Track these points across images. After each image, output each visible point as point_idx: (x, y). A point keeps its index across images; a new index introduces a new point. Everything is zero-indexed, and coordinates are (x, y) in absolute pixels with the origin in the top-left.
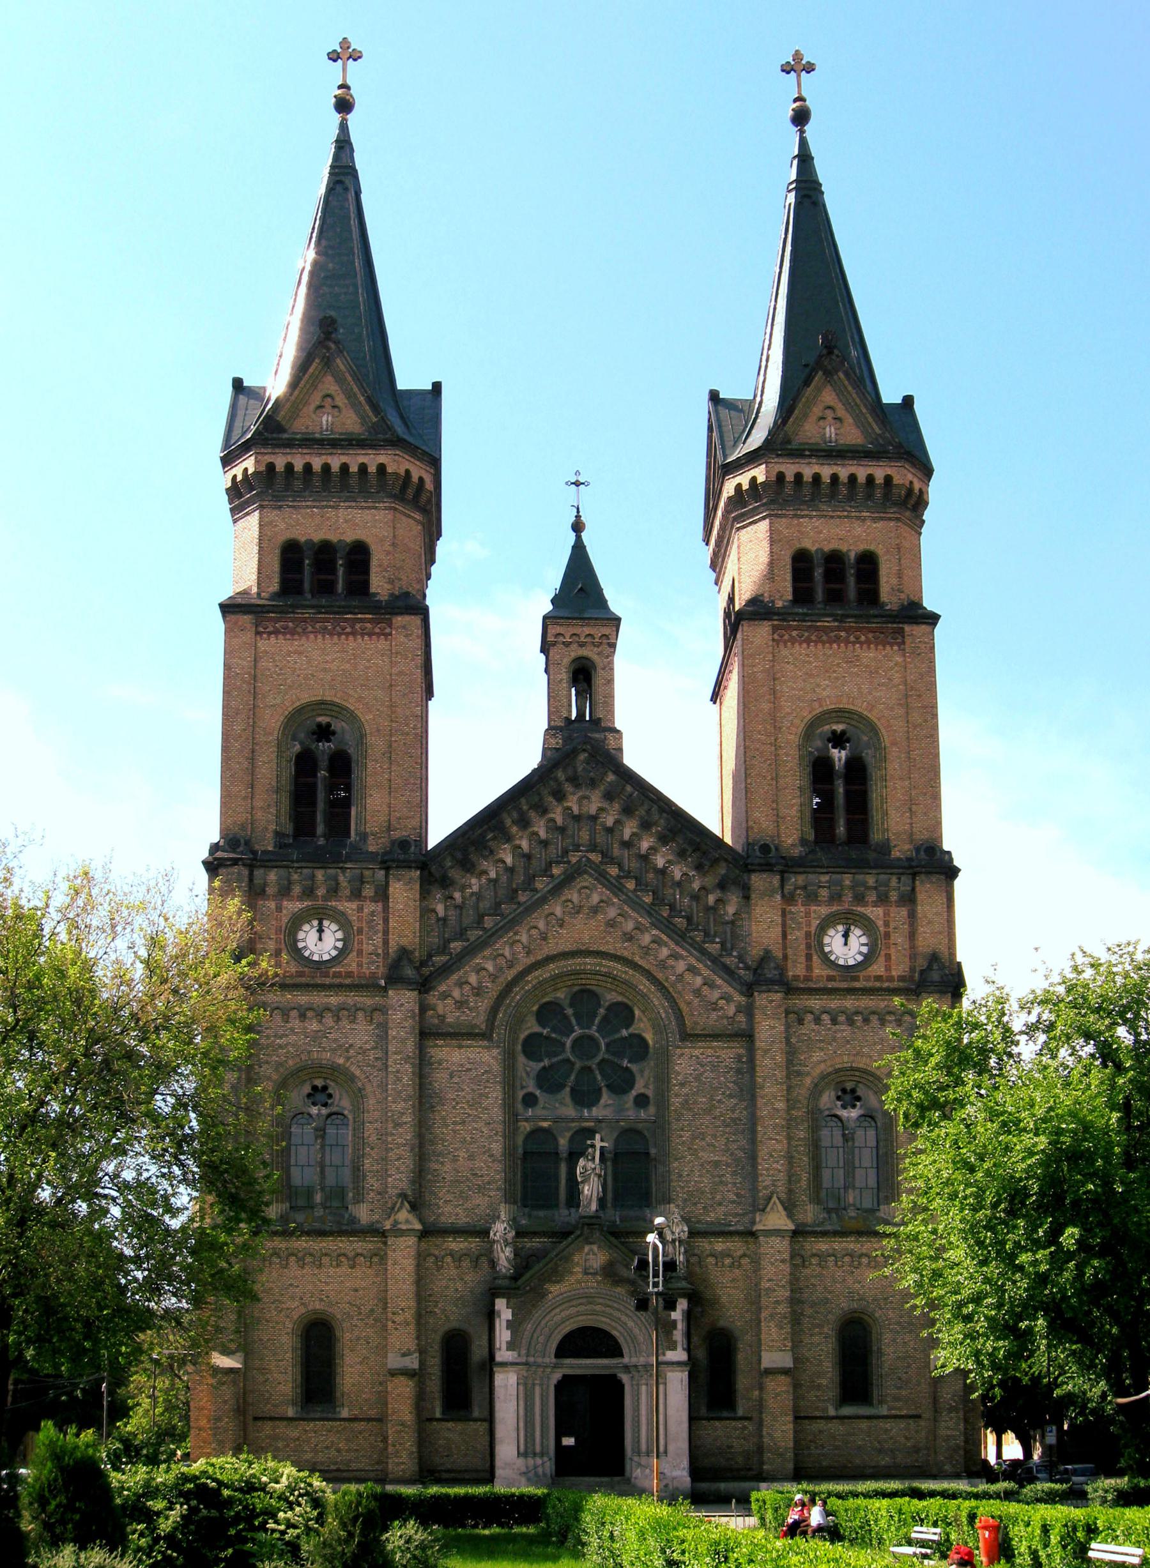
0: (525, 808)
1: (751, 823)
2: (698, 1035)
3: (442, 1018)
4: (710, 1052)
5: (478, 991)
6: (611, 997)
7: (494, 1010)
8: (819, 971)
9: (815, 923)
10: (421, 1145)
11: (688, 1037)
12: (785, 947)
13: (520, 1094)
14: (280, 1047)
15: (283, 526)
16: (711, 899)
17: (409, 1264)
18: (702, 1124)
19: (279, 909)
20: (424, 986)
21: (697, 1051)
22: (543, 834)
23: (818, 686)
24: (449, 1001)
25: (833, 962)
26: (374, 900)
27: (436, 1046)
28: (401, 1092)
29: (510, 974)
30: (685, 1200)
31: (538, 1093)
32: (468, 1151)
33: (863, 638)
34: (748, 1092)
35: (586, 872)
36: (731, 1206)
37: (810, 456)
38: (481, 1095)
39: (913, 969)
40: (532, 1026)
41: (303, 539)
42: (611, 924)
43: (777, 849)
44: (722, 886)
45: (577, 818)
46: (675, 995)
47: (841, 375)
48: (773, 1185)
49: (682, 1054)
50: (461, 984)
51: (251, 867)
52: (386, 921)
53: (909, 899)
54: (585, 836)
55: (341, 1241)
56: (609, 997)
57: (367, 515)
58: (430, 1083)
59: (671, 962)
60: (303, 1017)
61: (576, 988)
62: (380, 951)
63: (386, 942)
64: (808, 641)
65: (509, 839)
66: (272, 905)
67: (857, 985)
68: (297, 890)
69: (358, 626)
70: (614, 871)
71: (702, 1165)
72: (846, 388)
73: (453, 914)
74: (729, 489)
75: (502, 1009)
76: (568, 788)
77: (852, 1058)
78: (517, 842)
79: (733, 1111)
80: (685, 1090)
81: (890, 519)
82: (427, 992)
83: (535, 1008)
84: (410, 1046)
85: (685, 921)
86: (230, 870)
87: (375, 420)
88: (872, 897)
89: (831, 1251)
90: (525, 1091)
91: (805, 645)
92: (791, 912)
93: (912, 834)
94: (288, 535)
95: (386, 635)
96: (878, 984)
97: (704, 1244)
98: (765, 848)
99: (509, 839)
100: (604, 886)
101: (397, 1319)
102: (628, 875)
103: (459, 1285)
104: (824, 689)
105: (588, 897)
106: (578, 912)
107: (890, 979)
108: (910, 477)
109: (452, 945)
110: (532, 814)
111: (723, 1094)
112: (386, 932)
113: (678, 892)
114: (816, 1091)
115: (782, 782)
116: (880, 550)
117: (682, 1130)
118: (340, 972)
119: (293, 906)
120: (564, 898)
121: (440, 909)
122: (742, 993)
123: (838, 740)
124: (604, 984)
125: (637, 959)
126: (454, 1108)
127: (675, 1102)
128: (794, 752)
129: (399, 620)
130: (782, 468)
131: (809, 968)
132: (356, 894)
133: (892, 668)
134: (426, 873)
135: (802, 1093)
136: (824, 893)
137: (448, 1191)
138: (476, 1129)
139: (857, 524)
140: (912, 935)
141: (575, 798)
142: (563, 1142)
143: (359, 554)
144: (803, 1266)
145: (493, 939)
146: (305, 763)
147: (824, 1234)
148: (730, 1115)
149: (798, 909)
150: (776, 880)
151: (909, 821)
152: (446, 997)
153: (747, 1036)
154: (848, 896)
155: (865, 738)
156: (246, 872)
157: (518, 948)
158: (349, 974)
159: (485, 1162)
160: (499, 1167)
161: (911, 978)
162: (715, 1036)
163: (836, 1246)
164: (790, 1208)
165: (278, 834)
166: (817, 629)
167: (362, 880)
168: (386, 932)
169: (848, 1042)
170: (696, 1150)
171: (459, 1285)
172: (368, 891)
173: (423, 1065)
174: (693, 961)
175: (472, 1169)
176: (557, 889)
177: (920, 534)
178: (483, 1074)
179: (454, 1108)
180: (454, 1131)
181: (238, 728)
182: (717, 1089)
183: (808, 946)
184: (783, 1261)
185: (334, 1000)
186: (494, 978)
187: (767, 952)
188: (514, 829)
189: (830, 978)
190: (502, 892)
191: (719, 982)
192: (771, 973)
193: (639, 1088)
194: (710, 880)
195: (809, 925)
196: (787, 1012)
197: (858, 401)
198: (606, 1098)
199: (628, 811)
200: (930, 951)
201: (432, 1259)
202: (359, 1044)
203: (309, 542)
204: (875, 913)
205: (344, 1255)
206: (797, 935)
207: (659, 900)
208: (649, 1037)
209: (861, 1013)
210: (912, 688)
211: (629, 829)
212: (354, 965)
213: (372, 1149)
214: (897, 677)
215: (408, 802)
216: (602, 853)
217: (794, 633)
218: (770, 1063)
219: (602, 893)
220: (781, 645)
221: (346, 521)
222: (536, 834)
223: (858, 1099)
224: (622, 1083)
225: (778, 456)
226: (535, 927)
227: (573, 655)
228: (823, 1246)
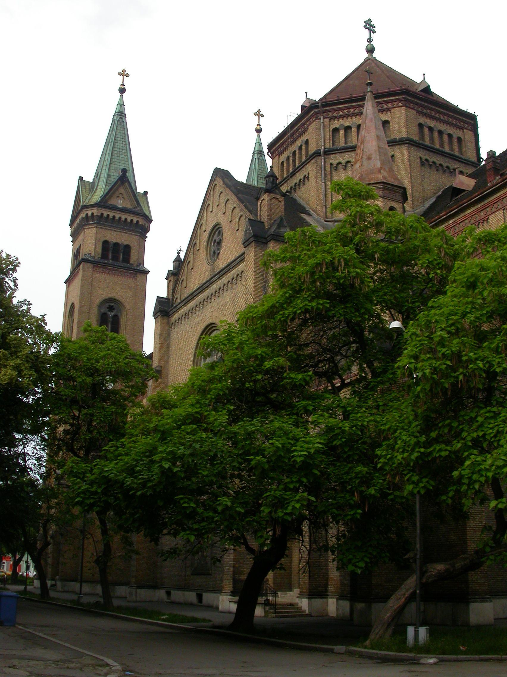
74: (83, 215)
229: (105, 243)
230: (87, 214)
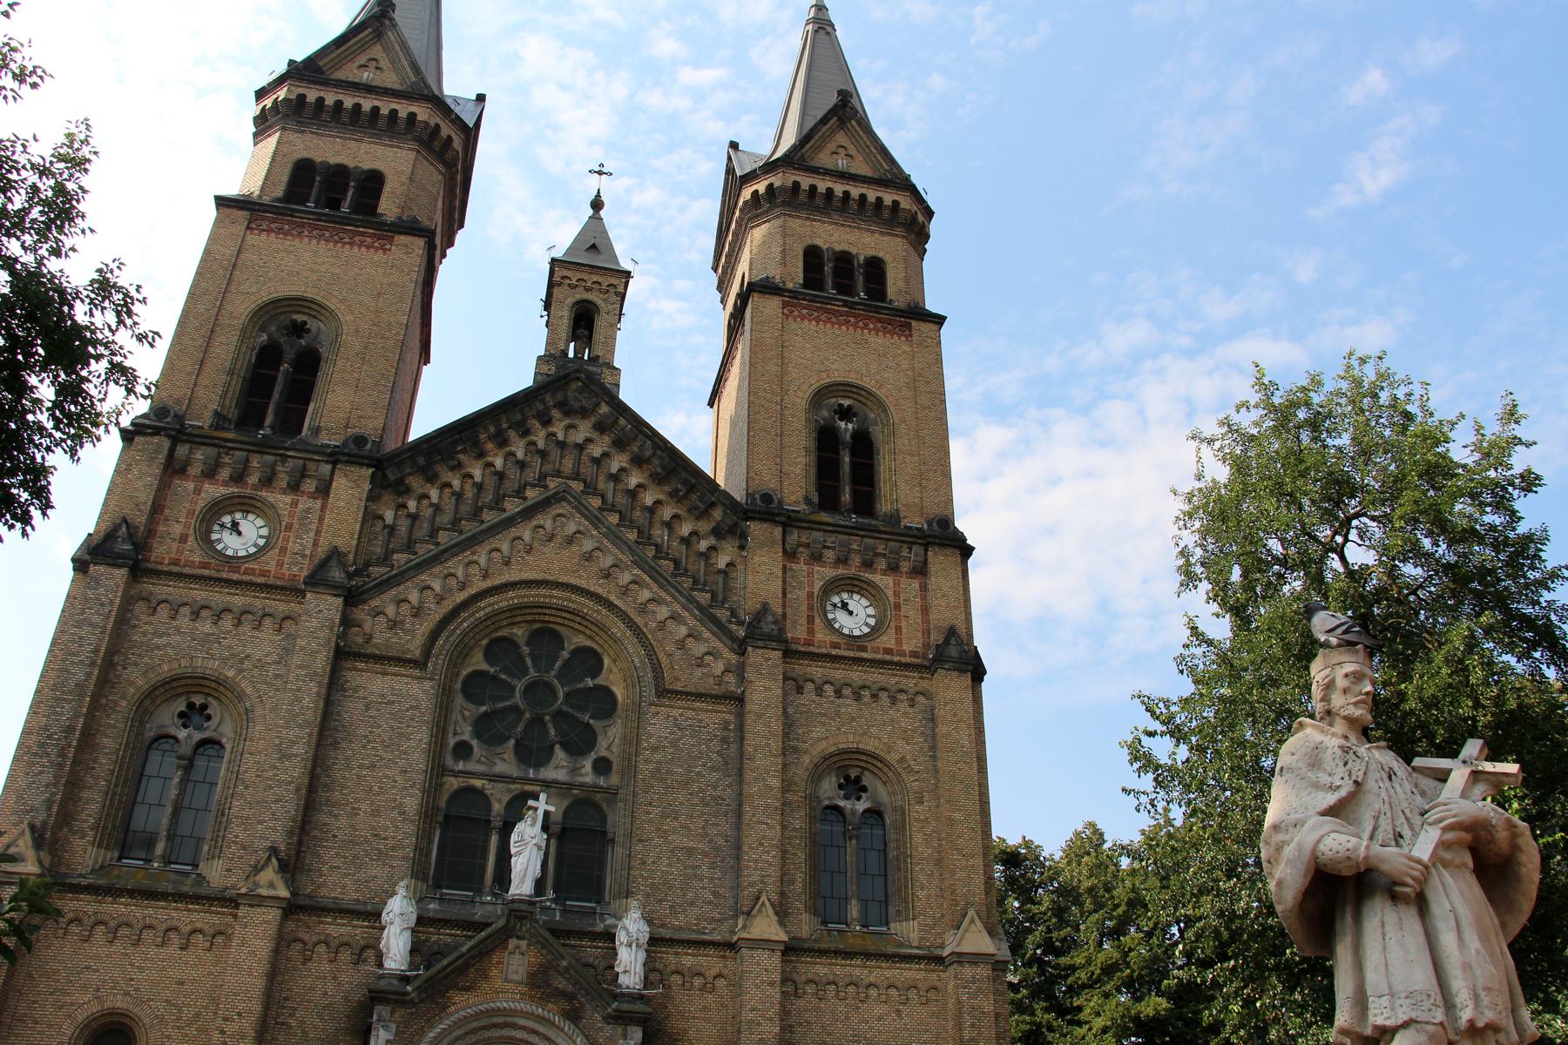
0: (505, 426)
1: (751, 474)
2: (677, 692)
4: (690, 713)
5: (417, 612)
6: (576, 640)
7: (434, 635)
8: (821, 635)
9: (818, 585)
10: (312, 788)
11: (664, 692)
12: (784, 606)
13: (452, 741)
14: (158, 647)
15: (300, 146)
16: (703, 545)
17: (261, 947)
19: (198, 491)
20: (352, 598)
21: (676, 710)
22: (520, 455)
23: (828, 359)
24: (381, 619)
25: (837, 630)
26: (313, 496)
27: (356, 669)
28: (297, 715)
29: (461, 597)
30: (648, 895)
31: (474, 743)
32: (372, 803)
33: (871, 326)
34: (737, 766)
35: (563, 499)
36: (707, 908)
37: (824, 174)
38: (401, 734)
39: (926, 646)
40: (478, 662)
41: (318, 160)
42: (588, 557)
43: (780, 502)
44: (717, 532)
45: (562, 445)
46: (655, 644)
47: (853, 123)
48: (762, 882)
49: (657, 713)
50: (400, 602)
51: (175, 441)
52: (321, 519)
53: (921, 571)
54: (568, 464)
55: (176, 909)
56: (576, 640)
57: (389, 152)
58: (339, 714)
59: (652, 606)
60: (196, 615)
61: (537, 626)
62: (308, 552)
63: (315, 544)
64: (818, 320)
65: (481, 455)
66: (191, 486)
67: (865, 655)
68: (225, 474)
69: (357, 238)
70: (596, 502)
71: (672, 851)
72: (857, 133)
73: (403, 526)
74: (746, 194)
75: (444, 635)
76: (556, 413)
77: (858, 738)
78: (490, 459)
80: (657, 757)
81: (897, 235)
82: (355, 605)
83: (484, 642)
84: (322, 662)
85: (672, 566)
86: (149, 439)
87: (414, 79)
88: (882, 564)
89: (831, 977)
90: (458, 738)
91: (814, 323)
92: (791, 569)
93: (922, 508)
94: (305, 155)
95: (385, 250)
96: (888, 657)
97: (670, 958)
98: (767, 498)
99: (481, 455)
100: (583, 515)
101: (230, 1028)
102: (612, 509)
103: (330, 987)
104: (832, 363)
105: (563, 526)
106: (550, 540)
107: (903, 654)
108: (916, 208)
109: (395, 557)
110: (512, 434)
111: (704, 765)
112: (318, 533)
113: (666, 533)
114: (817, 773)
115: (786, 440)
116: (888, 259)
118: (254, 569)
119: (215, 490)
120: (535, 523)
121: (389, 516)
122: (733, 650)
123: (845, 414)
124: (572, 624)
125: (612, 598)
126: (364, 747)
127: (644, 769)
128: (802, 415)
129: (401, 239)
130: (798, 179)
131: (811, 631)
132: (294, 487)
133: (899, 355)
134: (380, 474)
135: (801, 772)
136: (830, 555)
137: (338, 854)
138: (387, 777)
139: (866, 234)
140: (925, 610)
141: (562, 425)
142: (498, 808)
143: (373, 182)
144: (796, 995)
145: (447, 555)
146: (268, 356)
147: (823, 953)
148: (710, 791)
149: (800, 567)
150: (778, 531)
151: (919, 495)
152: (378, 614)
153: (740, 700)
154: (856, 560)
155: (872, 416)
156: (167, 443)
157: (474, 570)
158: (265, 573)
159: (393, 821)
160: (410, 828)
161: (925, 657)
162: (699, 696)
163: (838, 970)
164: (782, 914)
165: (217, 414)
166: (827, 311)
167: (303, 474)
168: (318, 533)
169: (853, 719)
170: (666, 832)
171: (330, 987)
172: (309, 486)
173: (334, 687)
174: (678, 608)
175: (373, 828)
176: (529, 512)
177: (923, 260)
178: (408, 710)
179: (364, 747)
181: (201, 308)
183: (810, 608)
184: (772, 984)
185: (238, 600)
186: (440, 599)
187: (765, 608)
188: (490, 446)
189: (835, 646)
190: (465, 509)
191: (706, 634)
192: (768, 627)
193: (602, 749)
194: (704, 526)
195: (811, 585)
196: (786, 678)
197: (868, 143)
198: (560, 754)
199: (620, 444)
200: (946, 625)
201: (299, 946)
202: (258, 654)
203: (325, 164)
204: (885, 582)
205: (176, 929)
206: (798, 594)
207: (645, 538)
208: (619, 692)
209: (869, 688)
210: (920, 375)
211: (617, 462)
212: (273, 563)
213: (246, 788)
214: (905, 365)
215: (374, 402)
216: (585, 482)
217: (804, 311)
218: (763, 732)
219: (580, 524)
220: (791, 319)
221: (367, 153)
222: (513, 454)
223: (864, 789)
224: (580, 742)
225: (794, 169)
226: (498, 550)
227: (578, 297)
228: (822, 969)
229: (812, 256)
230: (756, 191)
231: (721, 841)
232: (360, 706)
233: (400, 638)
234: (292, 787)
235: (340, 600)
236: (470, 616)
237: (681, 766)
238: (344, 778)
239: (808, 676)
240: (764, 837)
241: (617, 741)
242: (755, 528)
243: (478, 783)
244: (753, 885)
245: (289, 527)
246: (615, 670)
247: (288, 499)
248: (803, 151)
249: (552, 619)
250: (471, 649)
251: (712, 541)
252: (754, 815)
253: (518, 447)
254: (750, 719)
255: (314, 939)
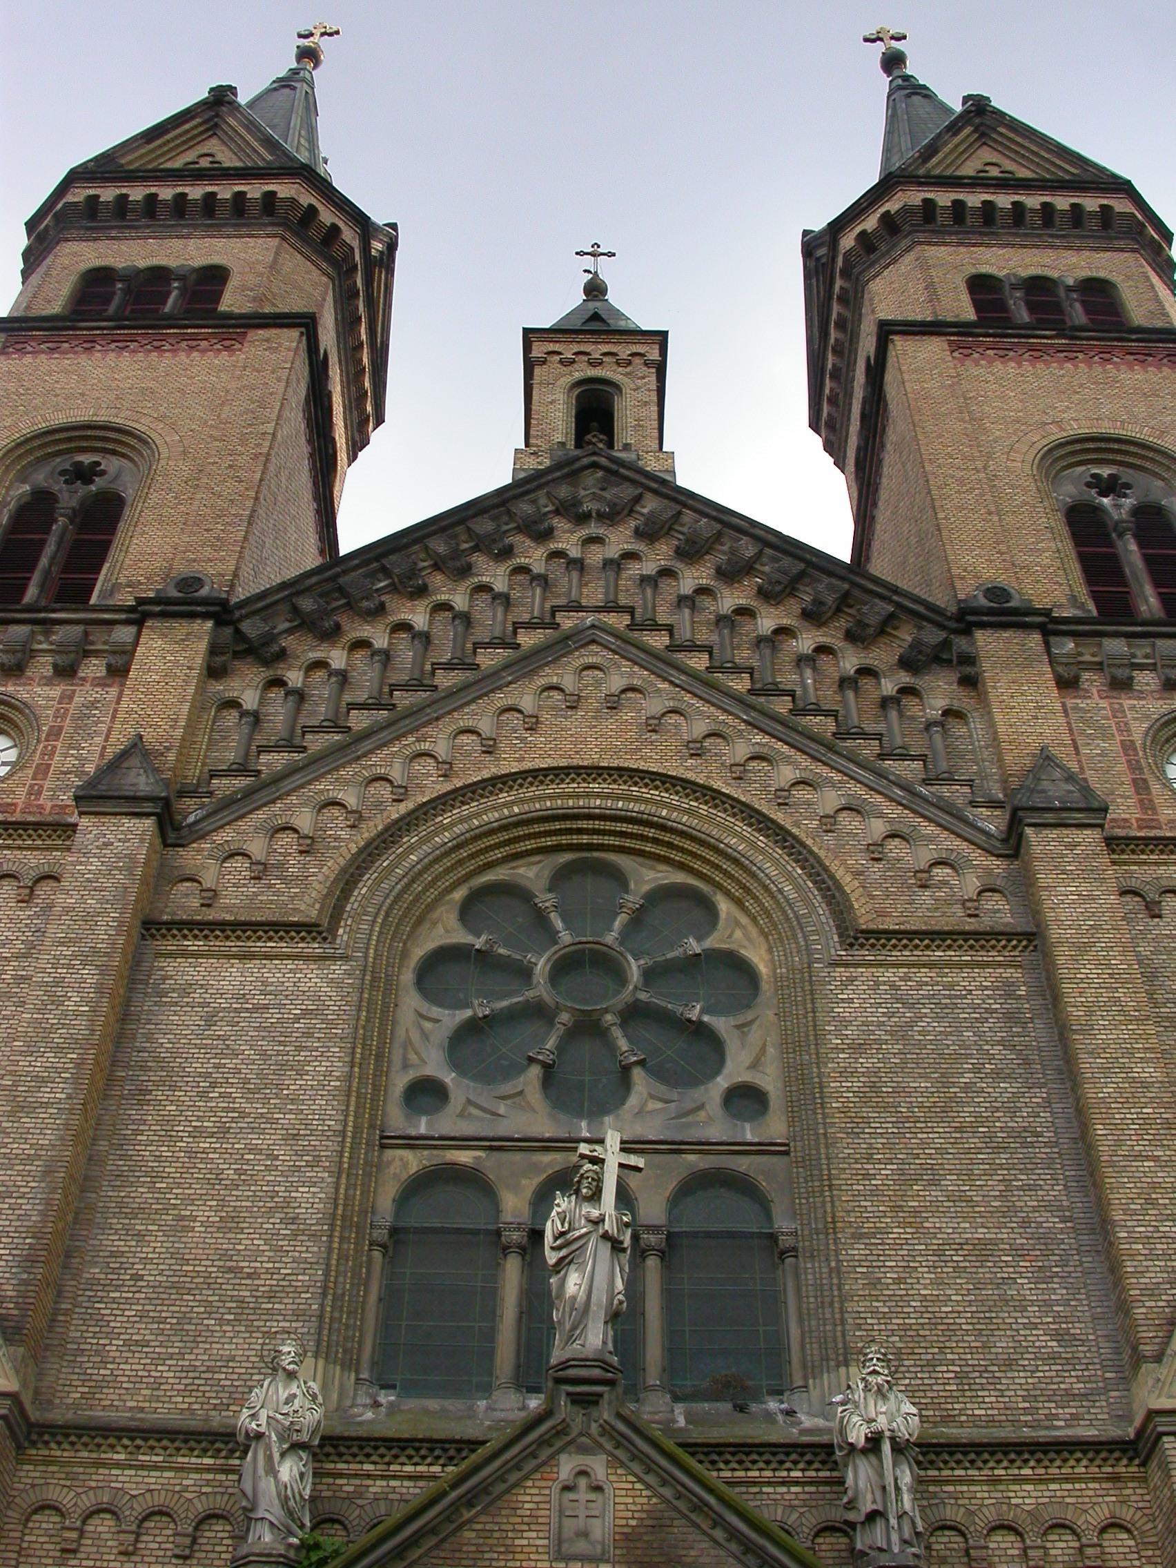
3: (211, 897)
4: (923, 974)
7: (348, 880)
9: (1138, 731)
13: (400, 1082)
18: (923, 1145)
24: (239, 863)
26: (101, 683)
27: (186, 954)
42: (654, 725)
46: (822, 854)
49: (852, 980)
57: (235, 243)
58: (149, 1037)
59: (801, 794)
75: (369, 878)
79: (1013, 1113)
81: (1122, 250)
90: (411, 1075)
92: (1076, 708)
109: (264, 758)
111: (976, 1070)
117: (869, 1158)
120: (542, 682)
124: (638, 845)
125: (717, 784)
132: (66, 672)
134: (228, 631)
137: (142, 1316)
159: (271, 1238)
160: (310, 1251)
170: (915, 1212)
175: (225, 1256)
178: (297, 1019)
179: (203, 1095)
180: (191, 1154)
182: (957, 1058)
191: (929, 829)
193: (735, 1071)
194: (883, 656)
195: (1125, 728)
201: (48, 1521)
208: (758, 957)
227: (578, 375)
231: (1052, 1222)
232: (194, 1019)
233: (278, 893)
234: (36, 1167)
235: (149, 823)
236: (422, 842)
237: (925, 1077)
238: (158, 1158)
239: (1164, 882)
240: (1154, 1186)
241: (771, 1050)
242: (986, 642)
243: (464, 1157)
244: (1152, 1292)
245: (55, 733)
246: (744, 920)
247: (55, 692)
248: (929, 165)
249: (596, 839)
250: (430, 908)
251: (905, 678)
252: (1119, 1143)
253: (495, 576)
254: (1062, 956)
255: (87, 1502)
